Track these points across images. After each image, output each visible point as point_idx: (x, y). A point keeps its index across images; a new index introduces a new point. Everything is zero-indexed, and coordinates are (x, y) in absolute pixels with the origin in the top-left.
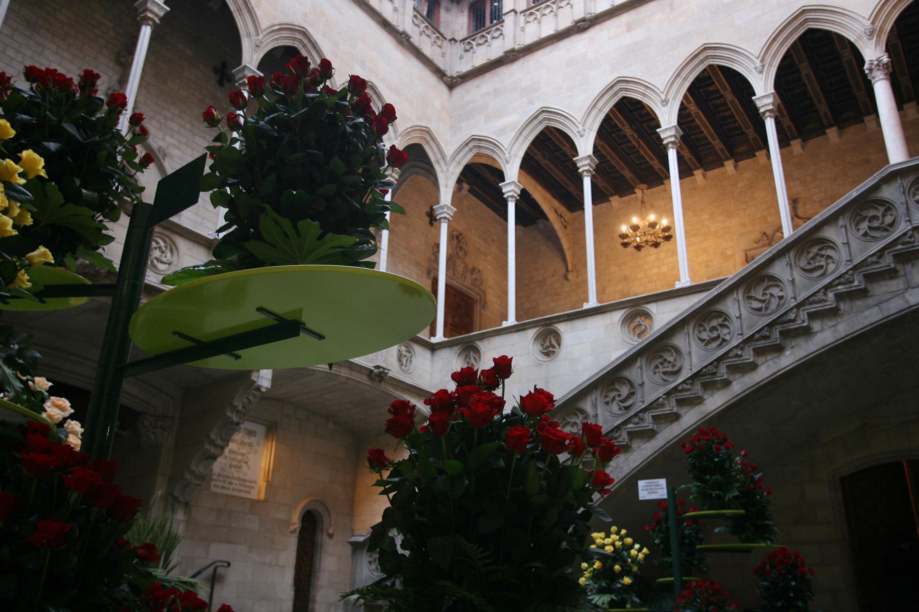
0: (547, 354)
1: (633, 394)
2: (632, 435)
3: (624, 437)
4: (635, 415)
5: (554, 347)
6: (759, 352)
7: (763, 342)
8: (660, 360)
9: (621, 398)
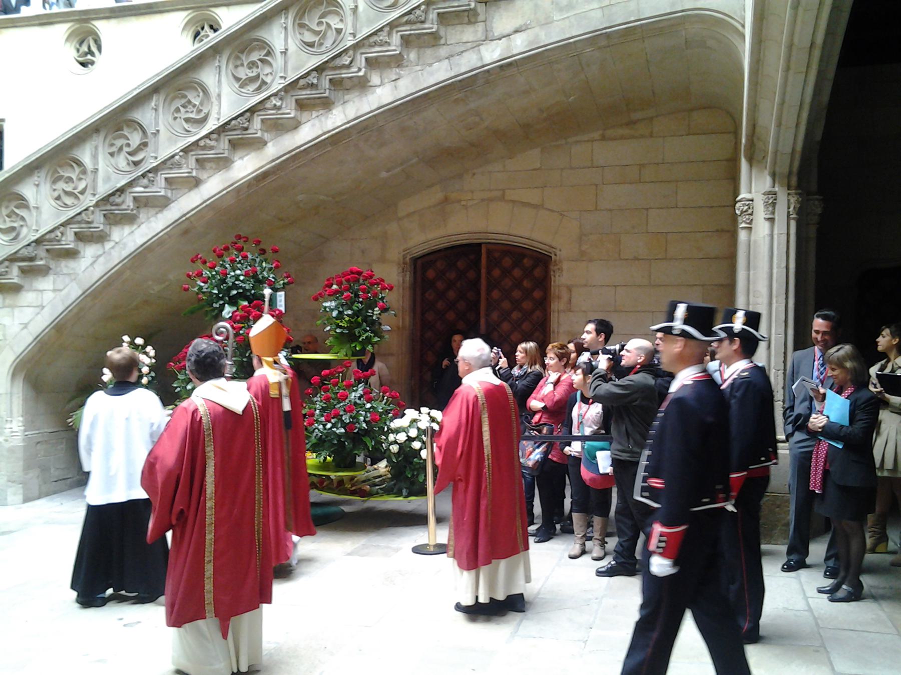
0: (83, 64)
1: (145, 145)
2: (142, 203)
3: (128, 202)
4: (143, 176)
5: (93, 54)
6: (301, 105)
8: (183, 101)
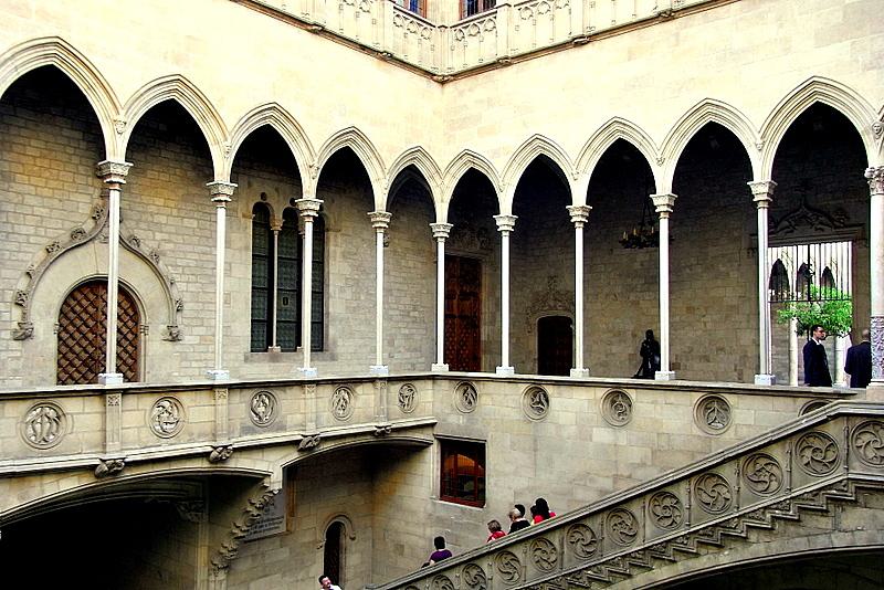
4: (594, 566)
7: (706, 538)
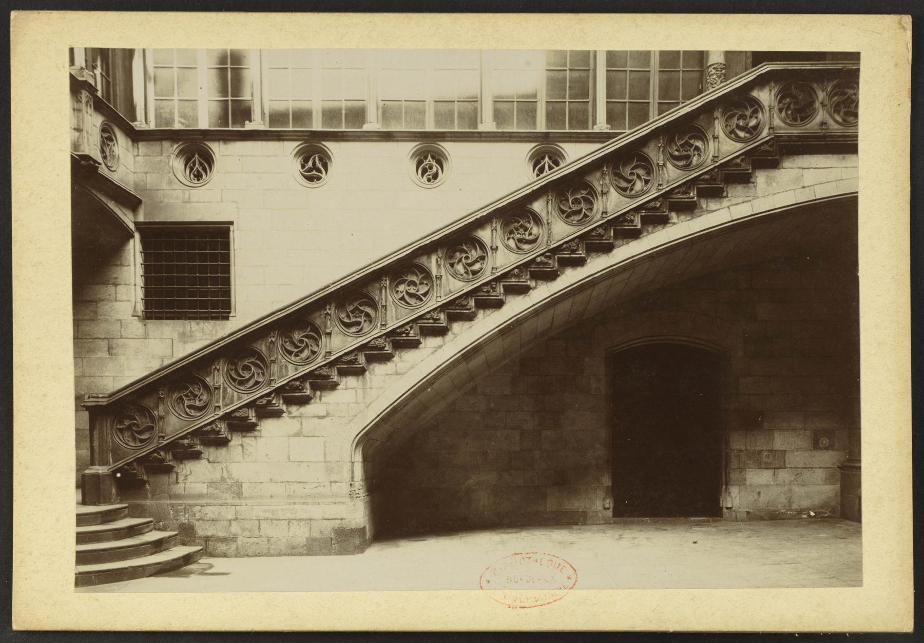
0: (310, 179)
9: (469, 261)
